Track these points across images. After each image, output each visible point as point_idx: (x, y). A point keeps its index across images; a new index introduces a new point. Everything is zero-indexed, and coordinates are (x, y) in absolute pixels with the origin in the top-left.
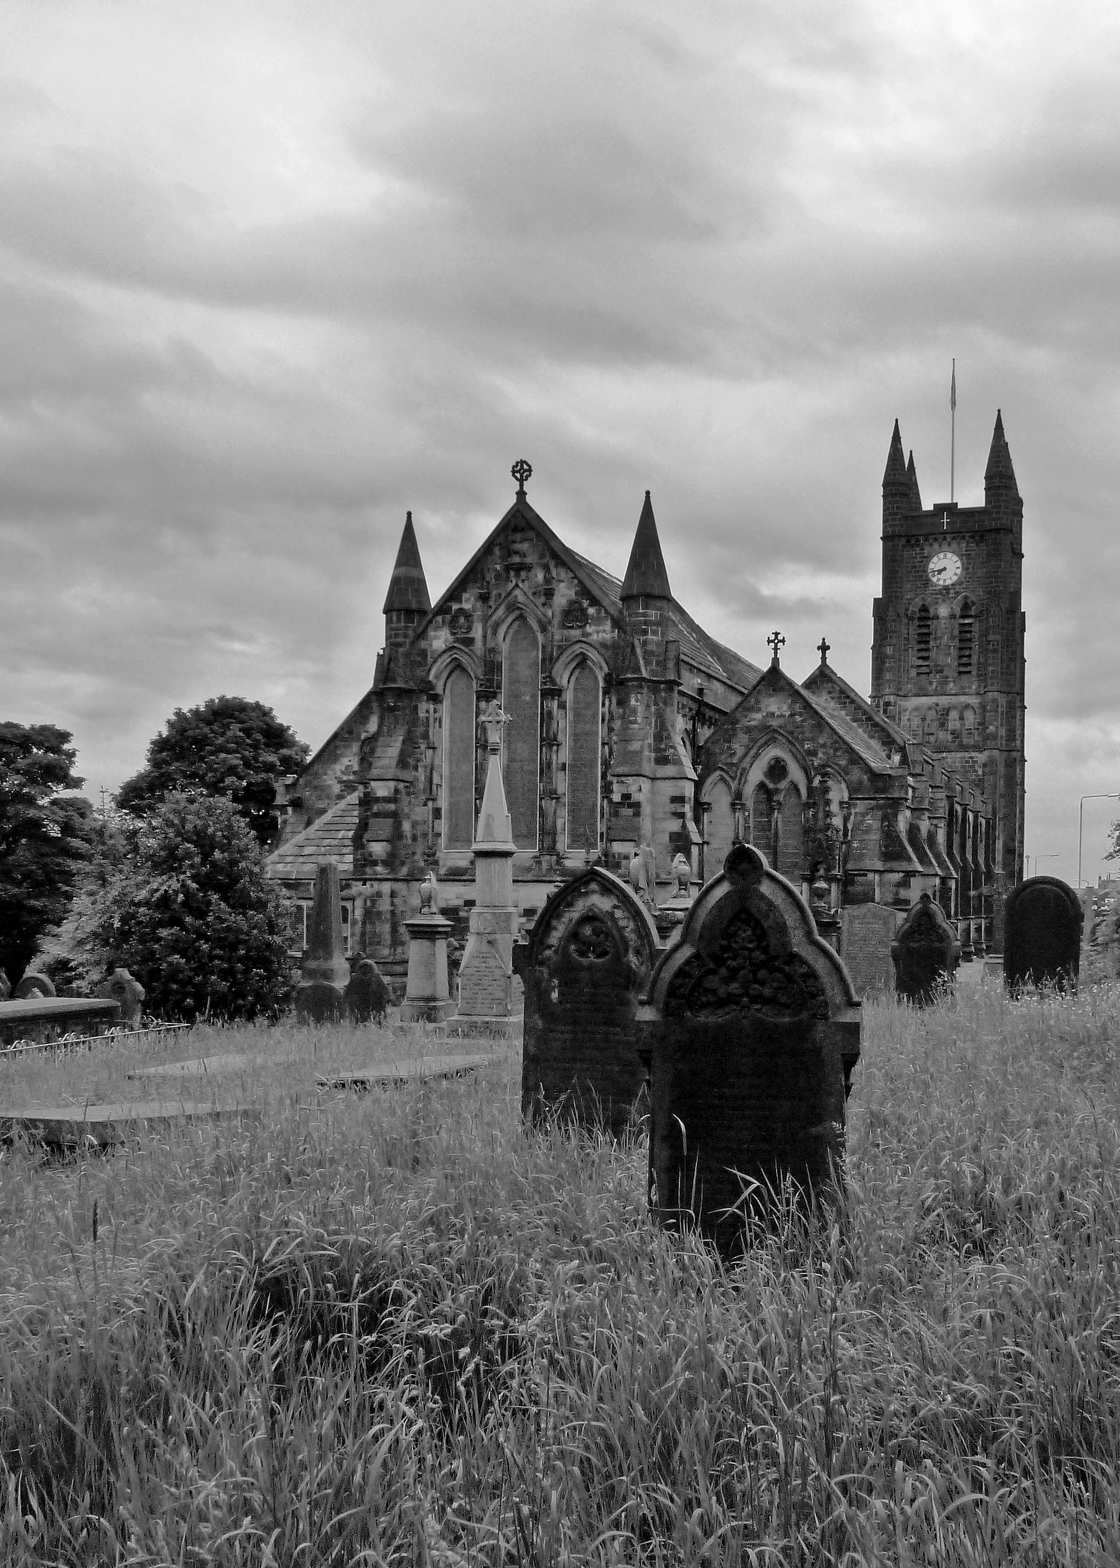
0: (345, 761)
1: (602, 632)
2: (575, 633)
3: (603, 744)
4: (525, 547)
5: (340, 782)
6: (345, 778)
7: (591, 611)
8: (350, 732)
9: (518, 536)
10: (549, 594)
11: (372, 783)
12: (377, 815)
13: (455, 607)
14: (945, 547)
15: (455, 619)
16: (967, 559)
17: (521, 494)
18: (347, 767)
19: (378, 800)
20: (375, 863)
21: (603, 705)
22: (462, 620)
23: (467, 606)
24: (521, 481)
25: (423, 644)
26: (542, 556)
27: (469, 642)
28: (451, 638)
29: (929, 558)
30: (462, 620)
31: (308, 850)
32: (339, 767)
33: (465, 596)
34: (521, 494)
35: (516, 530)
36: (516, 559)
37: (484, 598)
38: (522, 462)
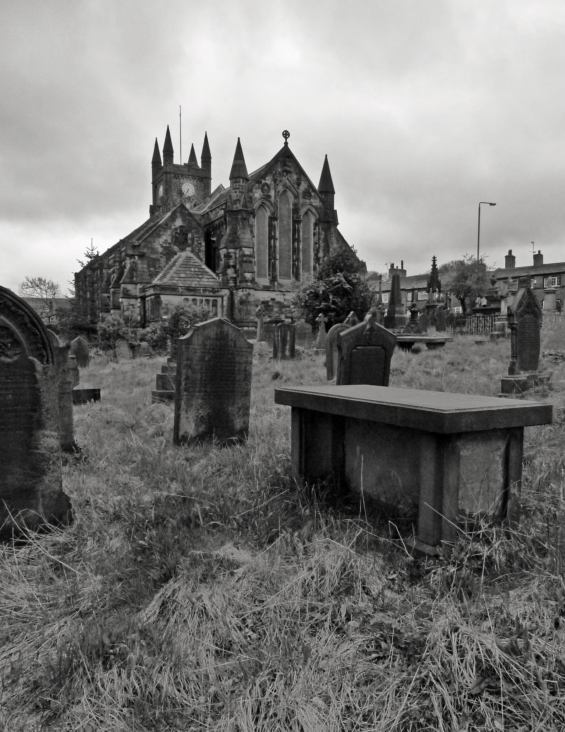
0: (164, 238)
1: (316, 202)
2: (308, 201)
3: (315, 243)
4: (289, 164)
5: (162, 246)
6: (164, 245)
7: (313, 194)
8: (166, 225)
9: (287, 159)
10: (299, 184)
11: (243, 249)
12: (246, 262)
13: (263, 182)
14: (188, 181)
15: (263, 186)
16: (196, 186)
17: (286, 143)
18: (166, 240)
19: (246, 256)
20: (247, 281)
21: (315, 229)
22: (266, 188)
23: (268, 182)
24: (286, 138)
25: (251, 194)
26: (295, 170)
27: (269, 197)
28: (262, 194)
29: (182, 184)
30: (266, 188)
31: (183, 275)
32: (161, 240)
33: (267, 178)
34: (286, 143)
35: (288, 157)
36: (288, 169)
37: (275, 181)
38: (286, 131)
